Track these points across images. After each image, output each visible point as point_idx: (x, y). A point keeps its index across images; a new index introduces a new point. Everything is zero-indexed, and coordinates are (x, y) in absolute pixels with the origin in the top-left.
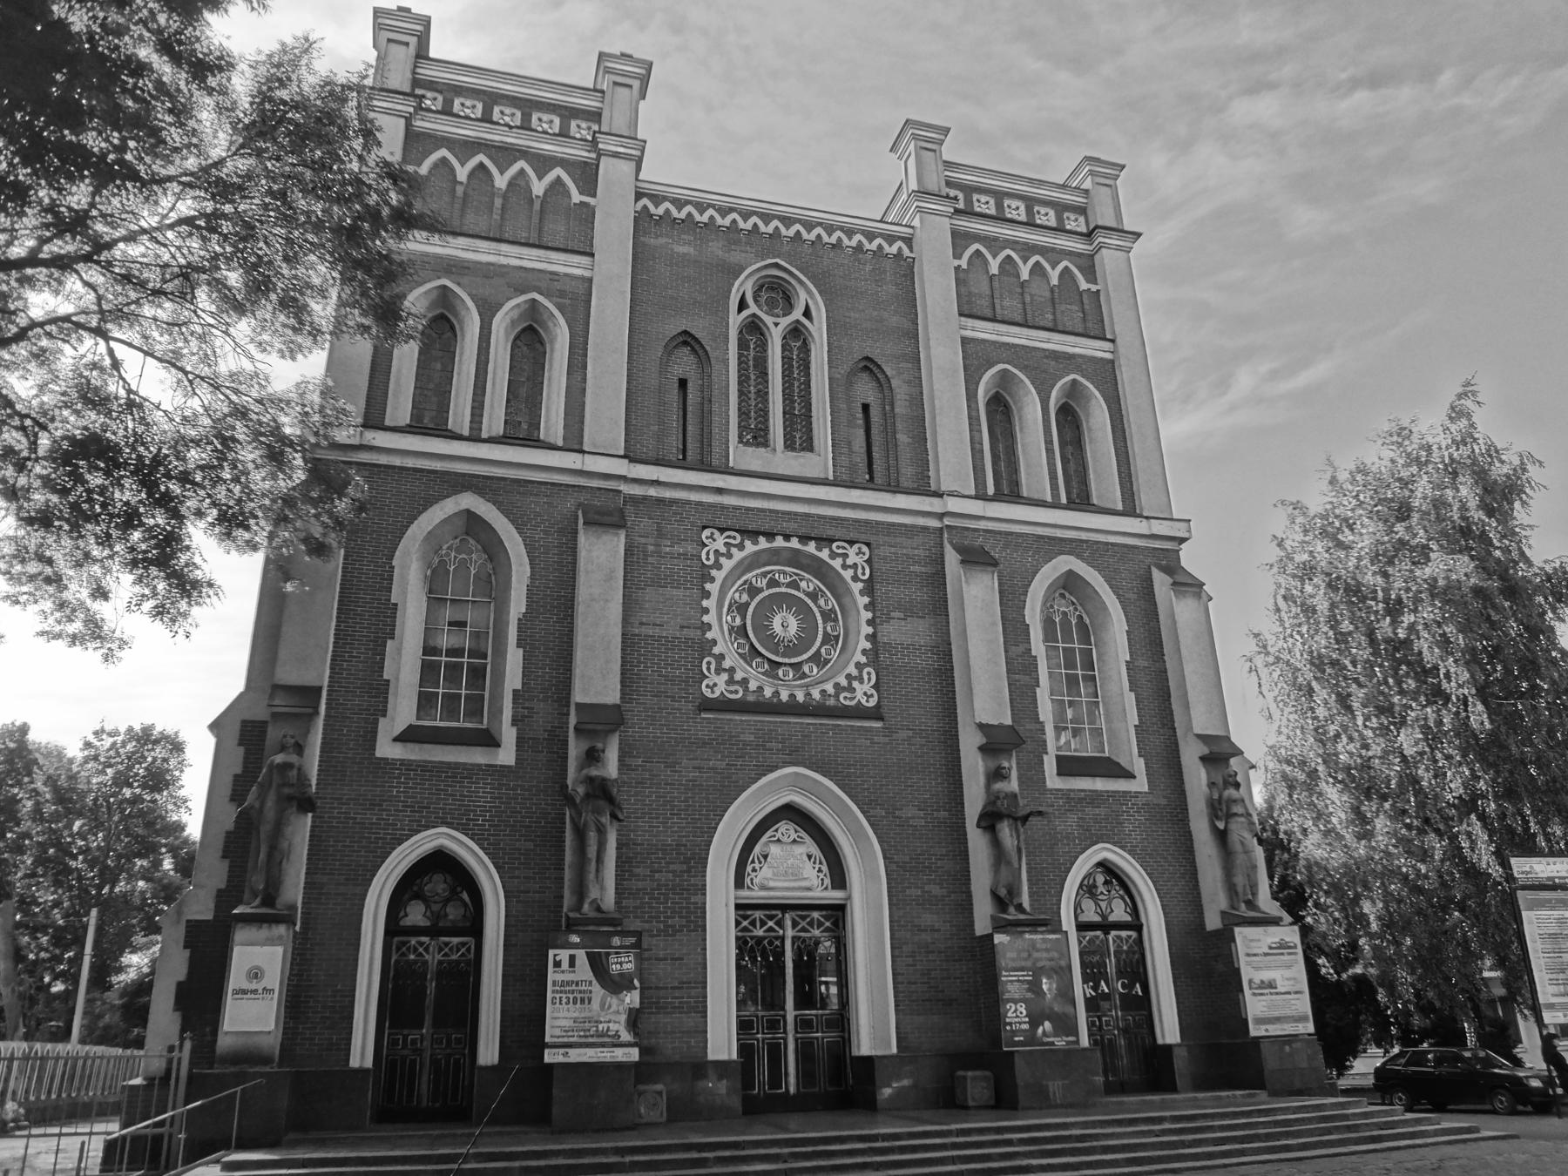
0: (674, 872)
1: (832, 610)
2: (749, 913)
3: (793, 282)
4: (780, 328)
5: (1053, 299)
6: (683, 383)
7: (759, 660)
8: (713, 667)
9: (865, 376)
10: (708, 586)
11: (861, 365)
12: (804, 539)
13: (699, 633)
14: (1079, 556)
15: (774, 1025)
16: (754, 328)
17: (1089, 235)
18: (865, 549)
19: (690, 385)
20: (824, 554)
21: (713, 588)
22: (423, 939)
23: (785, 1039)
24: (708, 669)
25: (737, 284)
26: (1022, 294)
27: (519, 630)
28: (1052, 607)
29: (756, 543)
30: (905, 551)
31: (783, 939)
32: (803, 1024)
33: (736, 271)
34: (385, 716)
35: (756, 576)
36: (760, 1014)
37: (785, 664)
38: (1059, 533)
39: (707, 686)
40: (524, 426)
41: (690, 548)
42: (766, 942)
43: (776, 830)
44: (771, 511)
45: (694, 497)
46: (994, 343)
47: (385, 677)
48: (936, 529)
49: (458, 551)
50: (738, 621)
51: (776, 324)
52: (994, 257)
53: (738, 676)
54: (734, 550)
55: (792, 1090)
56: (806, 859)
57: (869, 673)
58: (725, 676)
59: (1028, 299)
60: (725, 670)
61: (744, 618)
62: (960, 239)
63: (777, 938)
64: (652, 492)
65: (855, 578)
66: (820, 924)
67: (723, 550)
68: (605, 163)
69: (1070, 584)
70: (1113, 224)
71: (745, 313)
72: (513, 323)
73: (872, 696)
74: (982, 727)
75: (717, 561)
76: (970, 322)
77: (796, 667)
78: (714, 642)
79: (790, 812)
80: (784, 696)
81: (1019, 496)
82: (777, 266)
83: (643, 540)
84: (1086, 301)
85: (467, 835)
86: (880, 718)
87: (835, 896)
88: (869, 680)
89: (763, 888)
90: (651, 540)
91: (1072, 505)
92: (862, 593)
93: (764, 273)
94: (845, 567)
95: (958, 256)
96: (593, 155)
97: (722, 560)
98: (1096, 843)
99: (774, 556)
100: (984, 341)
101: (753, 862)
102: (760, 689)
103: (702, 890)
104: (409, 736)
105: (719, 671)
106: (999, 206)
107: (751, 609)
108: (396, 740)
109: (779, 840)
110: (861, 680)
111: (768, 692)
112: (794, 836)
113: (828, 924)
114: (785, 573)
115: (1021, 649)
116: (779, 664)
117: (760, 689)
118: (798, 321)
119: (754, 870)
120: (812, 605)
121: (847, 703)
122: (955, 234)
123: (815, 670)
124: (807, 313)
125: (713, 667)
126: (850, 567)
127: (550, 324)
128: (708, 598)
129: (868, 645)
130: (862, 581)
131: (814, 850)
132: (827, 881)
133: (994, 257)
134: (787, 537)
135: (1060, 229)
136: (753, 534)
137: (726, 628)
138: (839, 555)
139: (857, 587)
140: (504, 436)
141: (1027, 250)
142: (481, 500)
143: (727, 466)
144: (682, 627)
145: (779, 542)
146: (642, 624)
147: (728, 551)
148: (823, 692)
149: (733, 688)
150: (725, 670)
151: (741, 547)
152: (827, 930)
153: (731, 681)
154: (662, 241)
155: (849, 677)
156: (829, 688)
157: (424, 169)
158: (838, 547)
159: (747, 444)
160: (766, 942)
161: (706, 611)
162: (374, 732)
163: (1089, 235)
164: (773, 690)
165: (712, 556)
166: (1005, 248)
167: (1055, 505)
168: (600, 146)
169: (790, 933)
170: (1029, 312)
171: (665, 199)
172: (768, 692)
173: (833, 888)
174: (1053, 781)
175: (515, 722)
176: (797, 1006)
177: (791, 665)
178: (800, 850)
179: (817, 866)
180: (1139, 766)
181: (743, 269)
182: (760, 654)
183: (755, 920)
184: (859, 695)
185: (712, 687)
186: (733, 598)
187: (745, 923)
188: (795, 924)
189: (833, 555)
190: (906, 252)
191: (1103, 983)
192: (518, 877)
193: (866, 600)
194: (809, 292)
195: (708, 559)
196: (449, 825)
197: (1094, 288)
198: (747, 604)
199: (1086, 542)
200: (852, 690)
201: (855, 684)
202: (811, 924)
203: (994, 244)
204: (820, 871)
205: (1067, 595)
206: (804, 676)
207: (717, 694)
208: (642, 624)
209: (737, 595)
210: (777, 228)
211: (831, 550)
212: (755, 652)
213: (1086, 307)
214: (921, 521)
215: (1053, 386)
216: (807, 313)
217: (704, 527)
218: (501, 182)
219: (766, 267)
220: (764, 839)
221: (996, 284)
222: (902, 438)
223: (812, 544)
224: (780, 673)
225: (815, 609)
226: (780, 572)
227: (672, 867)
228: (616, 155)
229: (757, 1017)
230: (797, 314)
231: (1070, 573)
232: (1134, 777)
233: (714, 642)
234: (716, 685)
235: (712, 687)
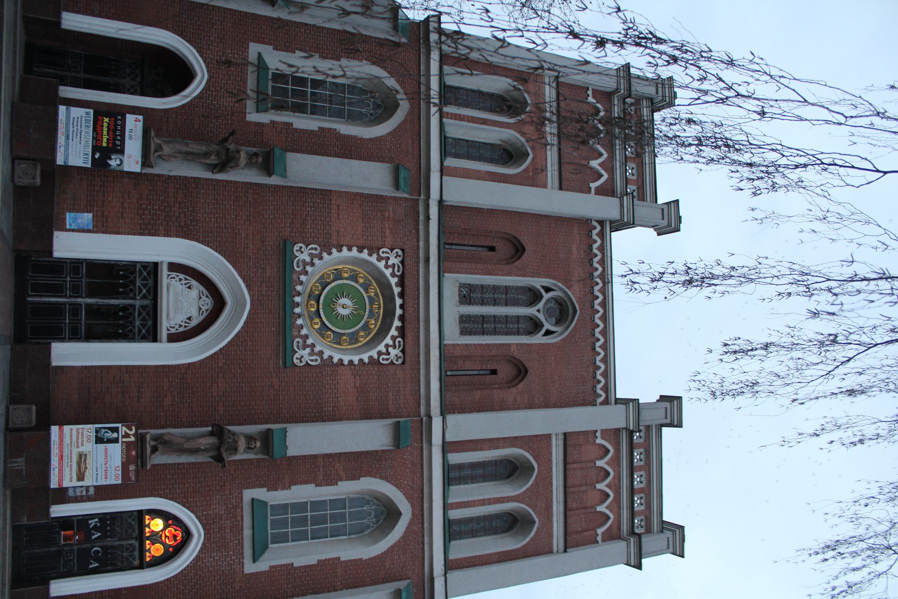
0: (179, 217)
1: (357, 341)
2: (152, 276)
3: (567, 323)
4: (537, 314)
5: (586, 508)
6: (492, 249)
7: (320, 288)
8: (313, 251)
9: (515, 372)
10: (366, 251)
11: (521, 368)
12: (402, 318)
13: (335, 242)
14: (411, 522)
15: (76, 291)
16: (534, 297)
17: (632, 533)
18: (400, 361)
19: (492, 253)
20: (393, 332)
21: (365, 255)
22: (139, 79)
23: (65, 296)
24: (312, 249)
25: (560, 284)
26: (586, 485)
27: (329, 129)
28: (374, 504)
29: (397, 285)
30: (402, 389)
31: (134, 298)
32: (75, 309)
33: (567, 282)
34: (274, 49)
35: (375, 289)
36: (84, 280)
37: (318, 306)
38: (426, 505)
39: (301, 247)
40: (453, 151)
41: (389, 241)
42: (132, 287)
43: (207, 297)
44: (418, 295)
45: (421, 244)
46: (550, 461)
47: (297, 52)
48: (419, 412)
49: (374, 103)
50: (346, 275)
51: (538, 311)
52: (607, 463)
53: (309, 268)
54: (390, 270)
55: (30, 299)
56: (188, 316)
57: (316, 360)
58: (308, 259)
59: (584, 488)
60: (312, 260)
61: (346, 279)
62: (614, 434)
63: (135, 295)
64: (422, 217)
65: (380, 353)
66: (144, 326)
67: (390, 263)
68: (615, 201)
69: (391, 514)
70: (643, 551)
72: (512, 145)
73: (301, 362)
74: (285, 431)
75: (382, 258)
76: (561, 442)
78: (330, 254)
79: (219, 303)
81: (449, 485)
82: (575, 311)
83: (391, 209)
84: (590, 533)
85: (203, 89)
87: (164, 334)
88: (312, 360)
90: (391, 215)
91: (448, 524)
92: (371, 357)
93: (569, 304)
94: (387, 346)
95: (606, 433)
96: (619, 196)
97: (384, 262)
98: (204, 529)
99: (389, 299)
100: (550, 453)
101: (186, 279)
102: (301, 283)
104: (261, 65)
105: (311, 255)
106: (640, 468)
107: (353, 283)
108: (259, 54)
109: (200, 298)
110: (312, 353)
111: (299, 288)
112: (204, 308)
113: (144, 331)
114: (379, 308)
115: (342, 473)
116: (318, 302)
117: (301, 283)
118: (542, 326)
119: (180, 280)
120: (359, 326)
121: (295, 343)
122: (617, 431)
123: (317, 327)
124: (548, 333)
125: (313, 251)
126: (387, 350)
127: (516, 166)
128: (358, 251)
129: (335, 360)
130: (379, 358)
131: (194, 323)
132: (173, 331)
133: (607, 463)
135: (633, 514)
136: (401, 283)
137: (340, 267)
138: (394, 342)
139: (374, 353)
140: (445, 137)
141: (615, 486)
142: (406, 113)
143: (444, 272)
144: (338, 232)
145: (399, 301)
146: (338, 206)
147: (389, 266)
148: (302, 327)
149: (301, 264)
150: (312, 260)
151: (393, 275)
152: (140, 331)
153: (305, 263)
154: (577, 237)
155: (313, 346)
156: (304, 332)
158: (399, 342)
159: (460, 291)
160: (132, 287)
161: (350, 249)
162: (264, 43)
163: (632, 533)
164: (301, 291)
165: (385, 255)
166: (614, 471)
167: (446, 507)
168: (625, 197)
169: (138, 303)
170: (577, 489)
171: (603, 241)
172: (299, 288)
173: (168, 334)
174: (248, 494)
175: (273, 122)
176: (87, 305)
177: (318, 310)
178: (194, 312)
179: (183, 324)
180: (263, 565)
181: (569, 287)
182: (323, 289)
183: (148, 280)
184: (300, 353)
185: (300, 250)
186: (360, 273)
187: (145, 273)
188: (143, 307)
189: (394, 338)
190: (600, 400)
191: (99, 534)
192: (176, 118)
193: (366, 360)
194: (562, 333)
195: (383, 252)
196: (209, 80)
197: (599, 538)
198: (357, 282)
199: (423, 527)
200: (305, 346)
201: (308, 350)
202: (144, 319)
204: (180, 326)
205: (383, 517)
206: (311, 319)
207: (297, 254)
208: (338, 206)
209: (362, 276)
210: (598, 312)
211: (397, 337)
213: (586, 534)
214: (423, 401)
215: (528, 505)
216: (548, 333)
217: (403, 250)
220: (202, 288)
221: (589, 465)
222: (478, 395)
223: (400, 324)
224: (313, 302)
225: (357, 327)
226: (379, 304)
227: (182, 215)
228: (622, 206)
229: (82, 278)
231: (399, 514)
232: (254, 561)
233: (330, 254)
235: (300, 250)
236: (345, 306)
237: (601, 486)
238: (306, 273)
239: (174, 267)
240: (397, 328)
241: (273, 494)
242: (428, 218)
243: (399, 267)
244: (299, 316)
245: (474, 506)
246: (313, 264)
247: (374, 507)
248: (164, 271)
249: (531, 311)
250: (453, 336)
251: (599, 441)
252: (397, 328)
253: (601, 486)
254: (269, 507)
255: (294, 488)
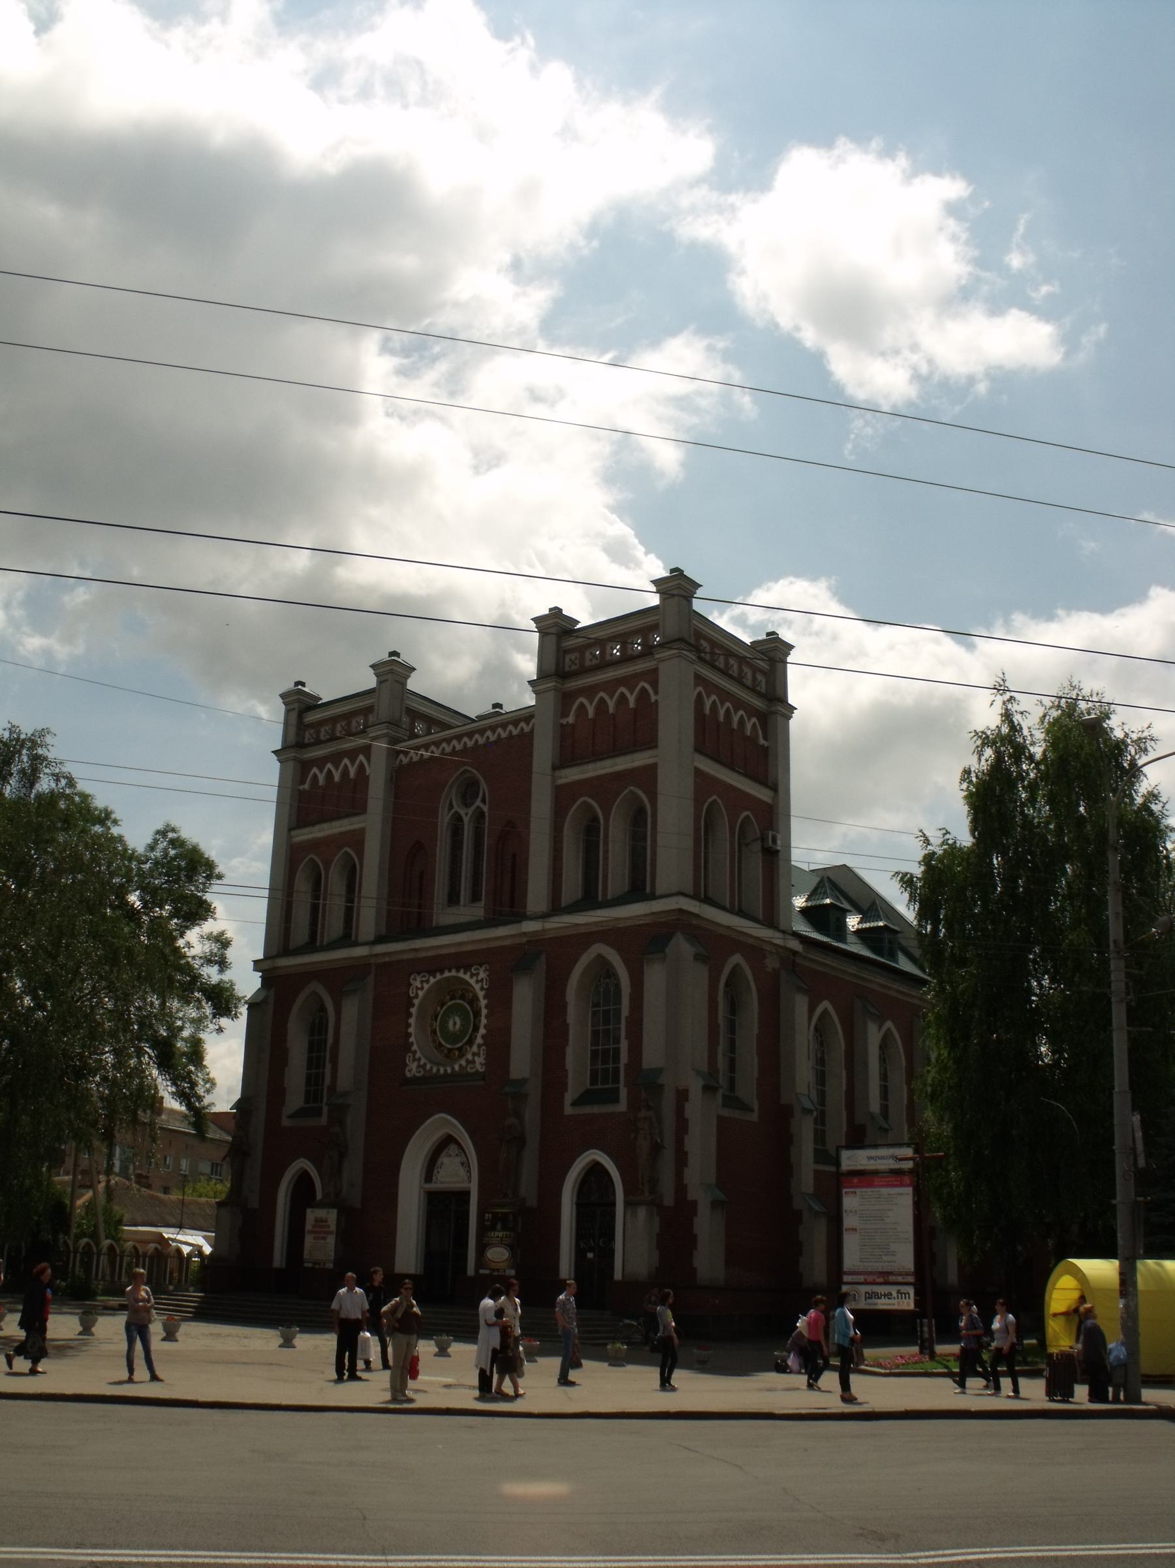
4: (469, 815)
12: (458, 971)
16: (458, 818)
20: (467, 977)
21: (413, 1010)
28: (599, 981)
39: (409, 1071)
51: (466, 814)
53: (422, 1063)
58: (416, 1064)
64: (387, 959)
65: (482, 989)
71: (452, 812)
77: (460, 1049)
80: (442, 1071)
86: (483, 1079)
89: (442, 1183)
94: (477, 982)
103: (396, 1185)
105: (414, 1060)
110: (478, 1054)
111: (435, 1070)
112: (457, 1152)
134: (450, 971)
136: (432, 973)
139: (481, 994)
145: (447, 974)
148: (461, 1066)
151: (428, 981)
153: (419, 1066)
155: (474, 1054)
157: (306, 786)
158: (475, 970)
165: (414, 991)
168: (370, 735)
172: (435, 1070)
174: (568, 1110)
178: (458, 1160)
180: (623, 1093)
191: (592, 1241)
200: (474, 1062)
201: (476, 1059)
203: (590, 691)
211: (472, 973)
212: (440, 1044)
216: (484, 801)
217: (410, 974)
218: (337, 777)
219: (461, 774)
220: (443, 1154)
223: (462, 971)
230: (478, 803)
234: (412, 1069)
236: (455, 1024)
237: (611, 704)
238: (425, 1064)
239: (429, 1176)
240: (465, 973)
241: (570, 1089)
242: (385, 954)
243: (423, 977)
244: (453, 1069)
245: (607, 869)
246: (419, 1059)
247: (602, 980)
248: (433, 1186)
249: (466, 819)
250: (477, 911)
251: (571, 719)
252: (465, 973)
253: (611, 704)
254: (592, 1087)
255: (567, 1068)
